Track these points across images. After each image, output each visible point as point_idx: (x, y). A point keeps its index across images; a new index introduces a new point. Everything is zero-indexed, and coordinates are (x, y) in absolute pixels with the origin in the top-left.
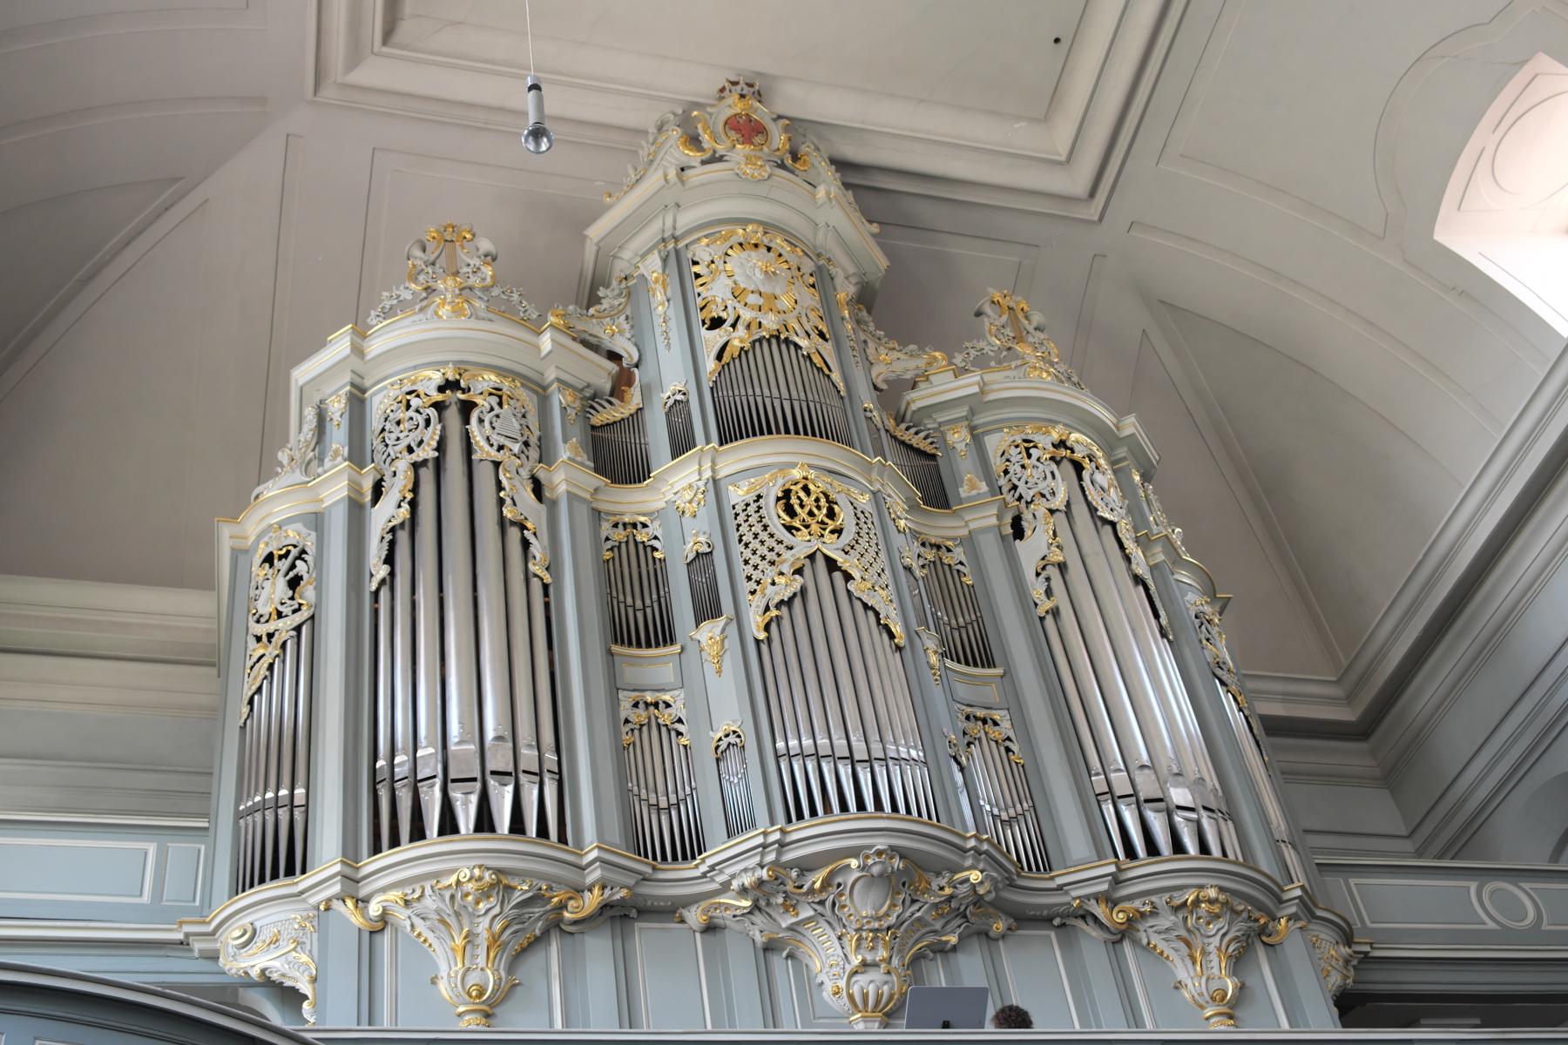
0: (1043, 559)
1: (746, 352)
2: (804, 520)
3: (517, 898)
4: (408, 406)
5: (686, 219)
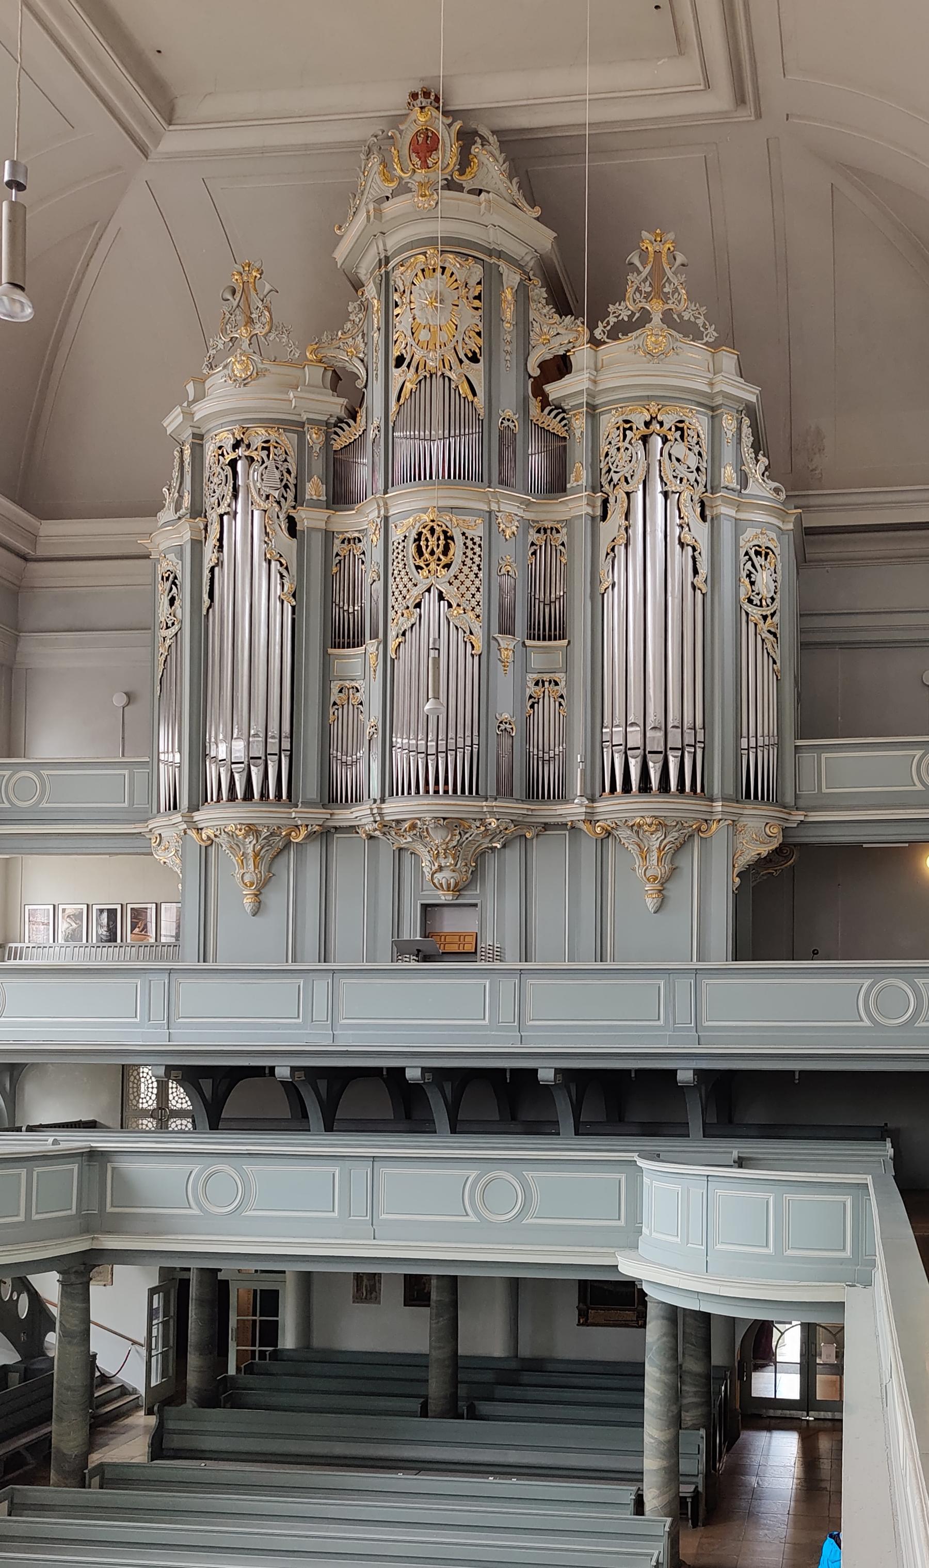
0: (613, 541)
1: (415, 392)
2: (427, 560)
5: (393, 242)
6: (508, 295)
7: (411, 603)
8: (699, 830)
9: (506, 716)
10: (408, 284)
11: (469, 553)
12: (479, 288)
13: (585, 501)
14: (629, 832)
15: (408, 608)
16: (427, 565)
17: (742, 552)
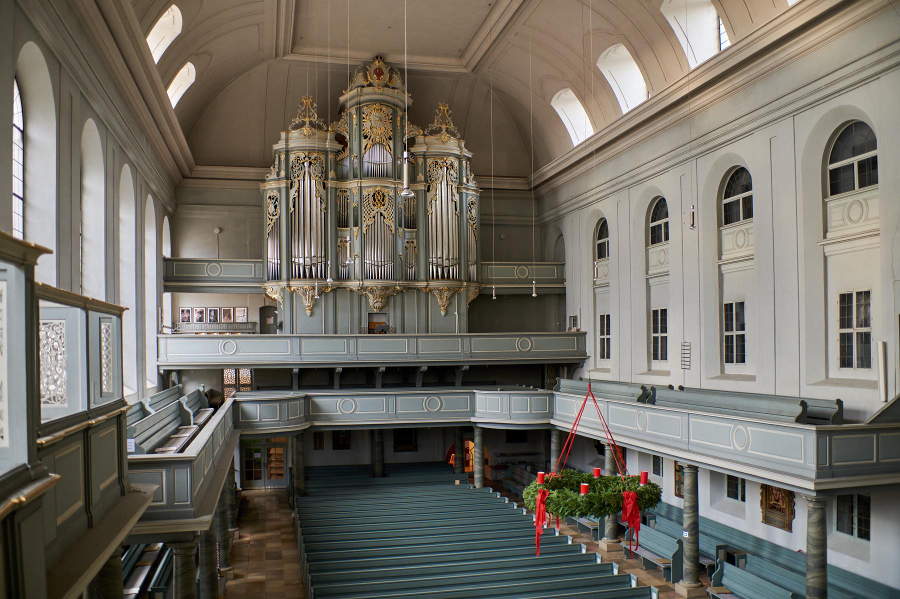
4: (298, 162)
5: (363, 98)
6: (399, 119)
7: (372, 216)
9: (401, 253)
11: (390, 201)
13: (423, 186)
14: (438, 291)
17: (468, 203)
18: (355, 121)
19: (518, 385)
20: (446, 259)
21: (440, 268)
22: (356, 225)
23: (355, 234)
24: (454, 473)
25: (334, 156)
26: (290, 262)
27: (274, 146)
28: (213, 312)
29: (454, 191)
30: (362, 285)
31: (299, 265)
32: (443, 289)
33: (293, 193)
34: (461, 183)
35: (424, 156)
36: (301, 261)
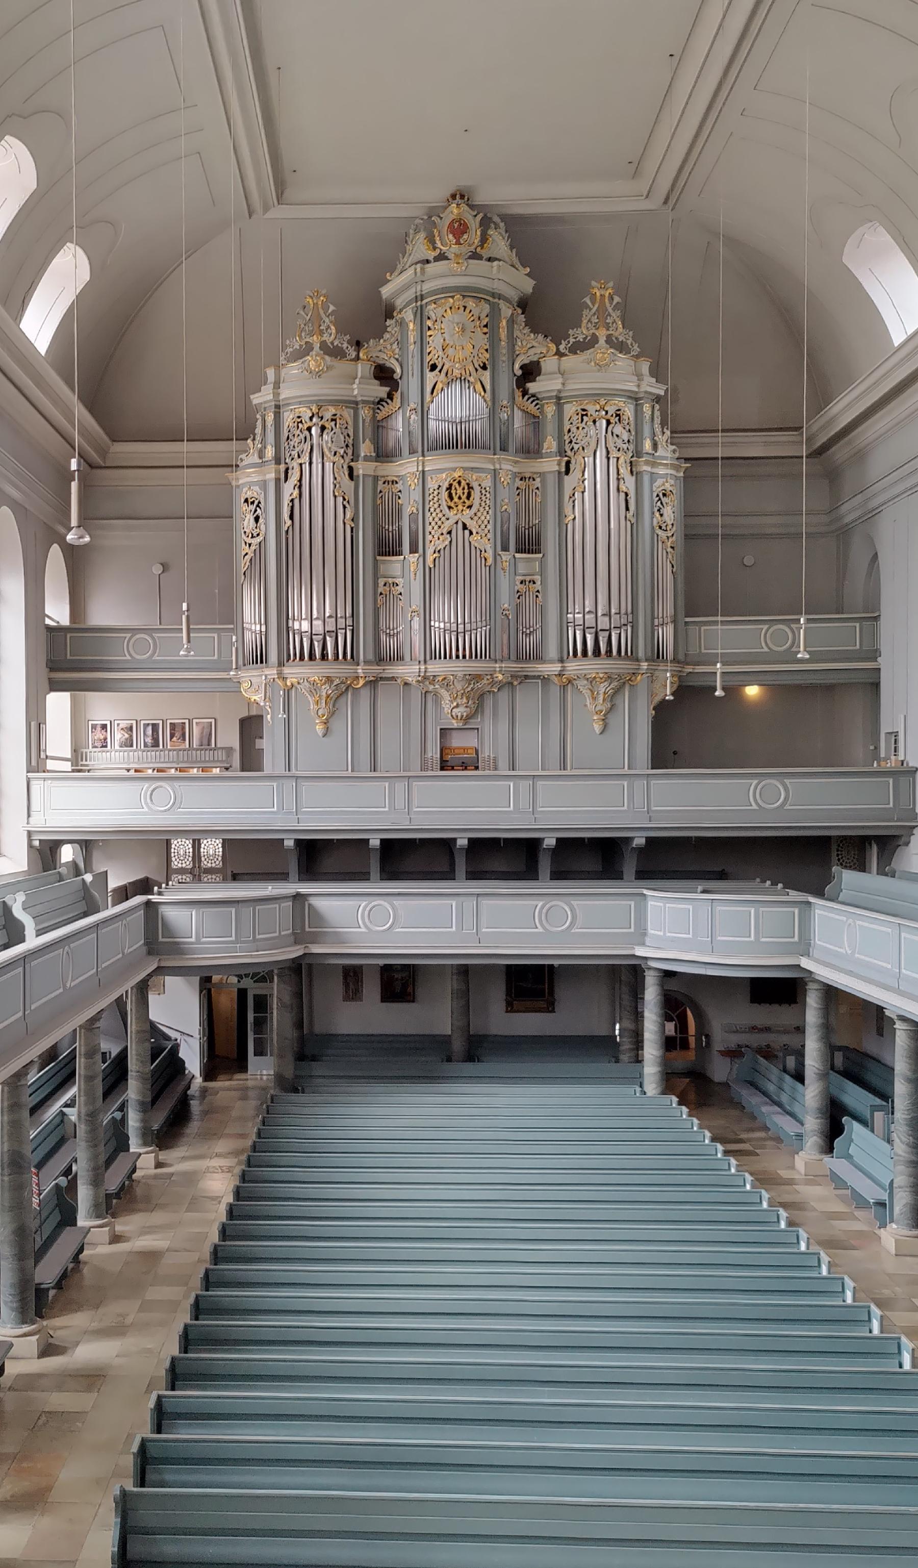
3: (335, 683)
5: (427, 287)
6: (504, 323)
7: (445, 532)
8: (630, 680)
9: (506, 606)
10: (440, 316)
11: (484, 498)
12: (487, 320)
13: (556, 462)
14: (586, 682)
15: (442, 534)
16: (457, 506)
18: (412, 336)
19: (758, 880)
20: (603, 615)
21: (590, 633)
22: (414, 550)
23: (412, 570)
24: (617, 1061)
25: (371, 411)
26: (284, 629)
27: (252, 397)
28: (150, 729)
29: (621, 471)
30: (425, 671)
31: (301, 634)
32: (595, 678)
33: (289, 490)
34: (638, 453)
35: (559, 398)
36: (305, 626)
